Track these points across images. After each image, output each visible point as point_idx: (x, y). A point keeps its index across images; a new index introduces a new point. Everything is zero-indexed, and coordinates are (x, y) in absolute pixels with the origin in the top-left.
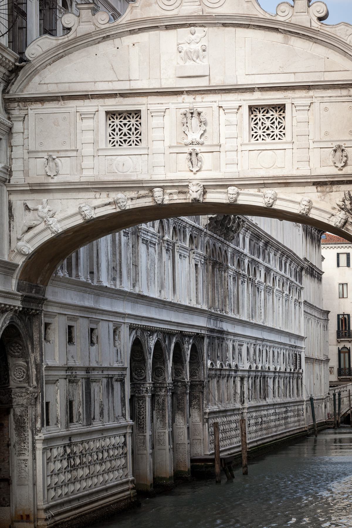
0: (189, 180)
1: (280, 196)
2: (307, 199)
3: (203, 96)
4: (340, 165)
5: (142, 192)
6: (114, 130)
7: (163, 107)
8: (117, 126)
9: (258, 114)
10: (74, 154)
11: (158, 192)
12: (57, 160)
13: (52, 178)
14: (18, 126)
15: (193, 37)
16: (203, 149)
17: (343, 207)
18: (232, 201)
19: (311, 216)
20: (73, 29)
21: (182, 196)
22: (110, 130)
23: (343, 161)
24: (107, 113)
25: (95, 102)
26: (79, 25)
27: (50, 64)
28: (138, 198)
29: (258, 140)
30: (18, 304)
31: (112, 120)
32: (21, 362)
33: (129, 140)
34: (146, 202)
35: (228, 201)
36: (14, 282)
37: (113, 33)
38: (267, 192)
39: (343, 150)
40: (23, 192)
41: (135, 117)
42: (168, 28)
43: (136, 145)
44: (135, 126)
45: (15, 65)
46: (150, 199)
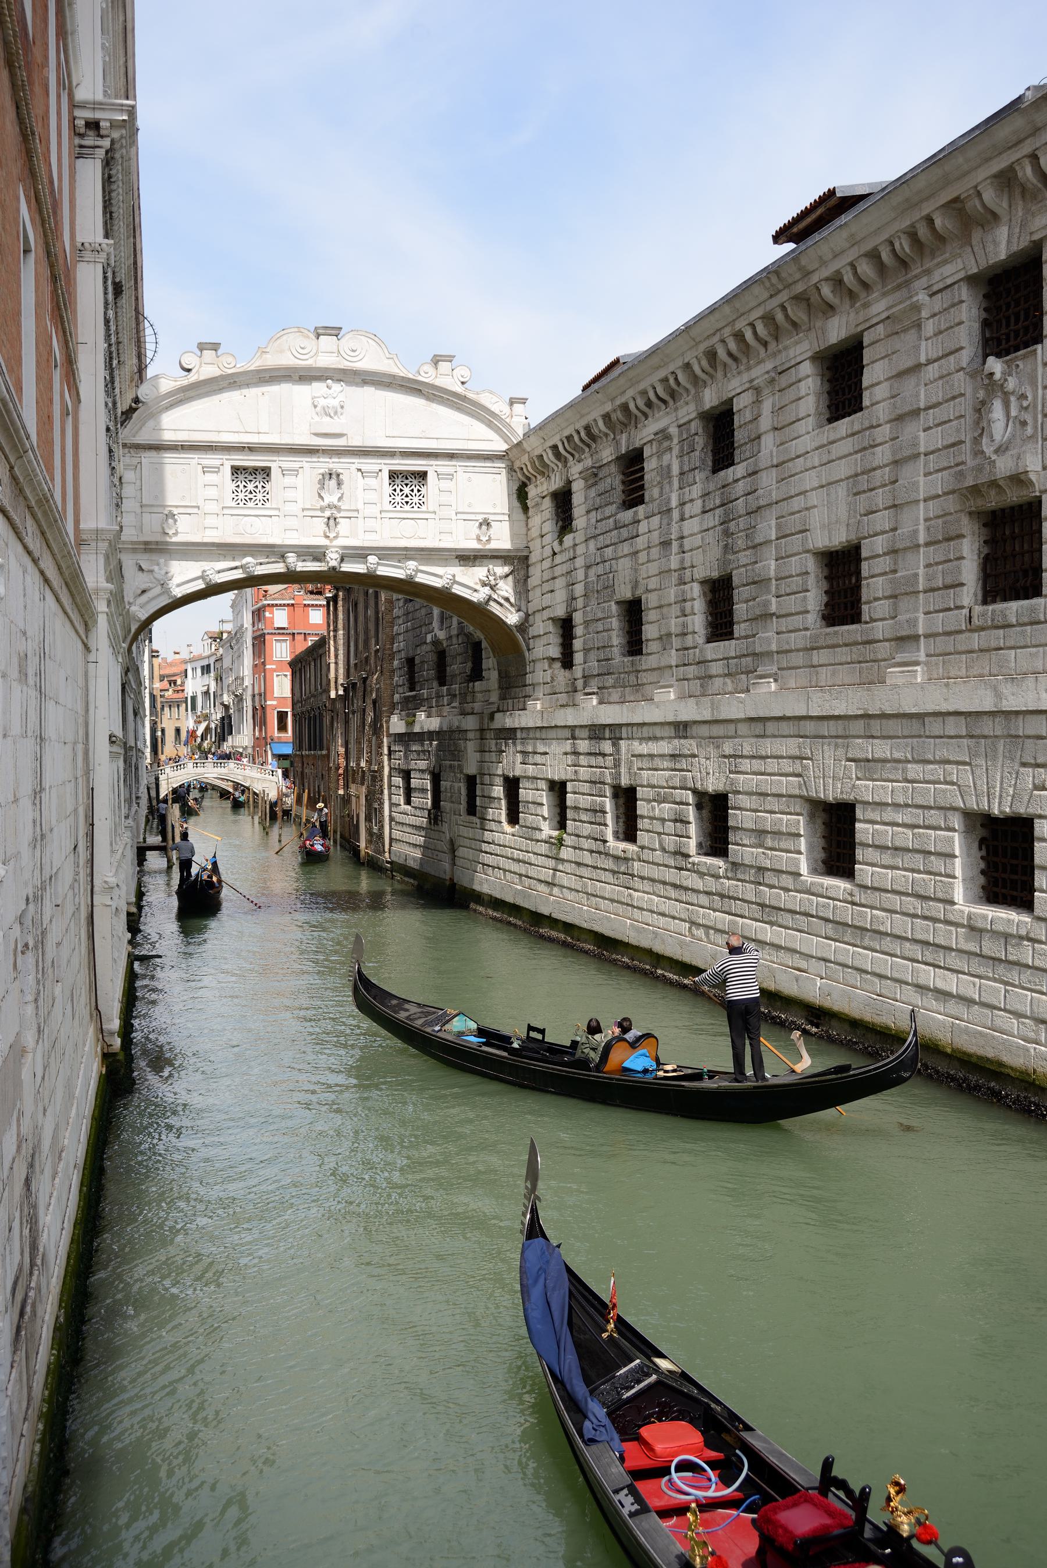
0: (326, 547)
4: (484, 539)
7: (296, 465)
10: (195, 510)
11: (291, 558)
14: (129, 476)
15: (331, 392)
16: (342, 514)
19: (453, 591)
21: (319, 564)
26: (200, 366)
28: (268, 563)
34: (279, 568)
39: (488, 524)
40: (134, 550)
46: (282, 565)
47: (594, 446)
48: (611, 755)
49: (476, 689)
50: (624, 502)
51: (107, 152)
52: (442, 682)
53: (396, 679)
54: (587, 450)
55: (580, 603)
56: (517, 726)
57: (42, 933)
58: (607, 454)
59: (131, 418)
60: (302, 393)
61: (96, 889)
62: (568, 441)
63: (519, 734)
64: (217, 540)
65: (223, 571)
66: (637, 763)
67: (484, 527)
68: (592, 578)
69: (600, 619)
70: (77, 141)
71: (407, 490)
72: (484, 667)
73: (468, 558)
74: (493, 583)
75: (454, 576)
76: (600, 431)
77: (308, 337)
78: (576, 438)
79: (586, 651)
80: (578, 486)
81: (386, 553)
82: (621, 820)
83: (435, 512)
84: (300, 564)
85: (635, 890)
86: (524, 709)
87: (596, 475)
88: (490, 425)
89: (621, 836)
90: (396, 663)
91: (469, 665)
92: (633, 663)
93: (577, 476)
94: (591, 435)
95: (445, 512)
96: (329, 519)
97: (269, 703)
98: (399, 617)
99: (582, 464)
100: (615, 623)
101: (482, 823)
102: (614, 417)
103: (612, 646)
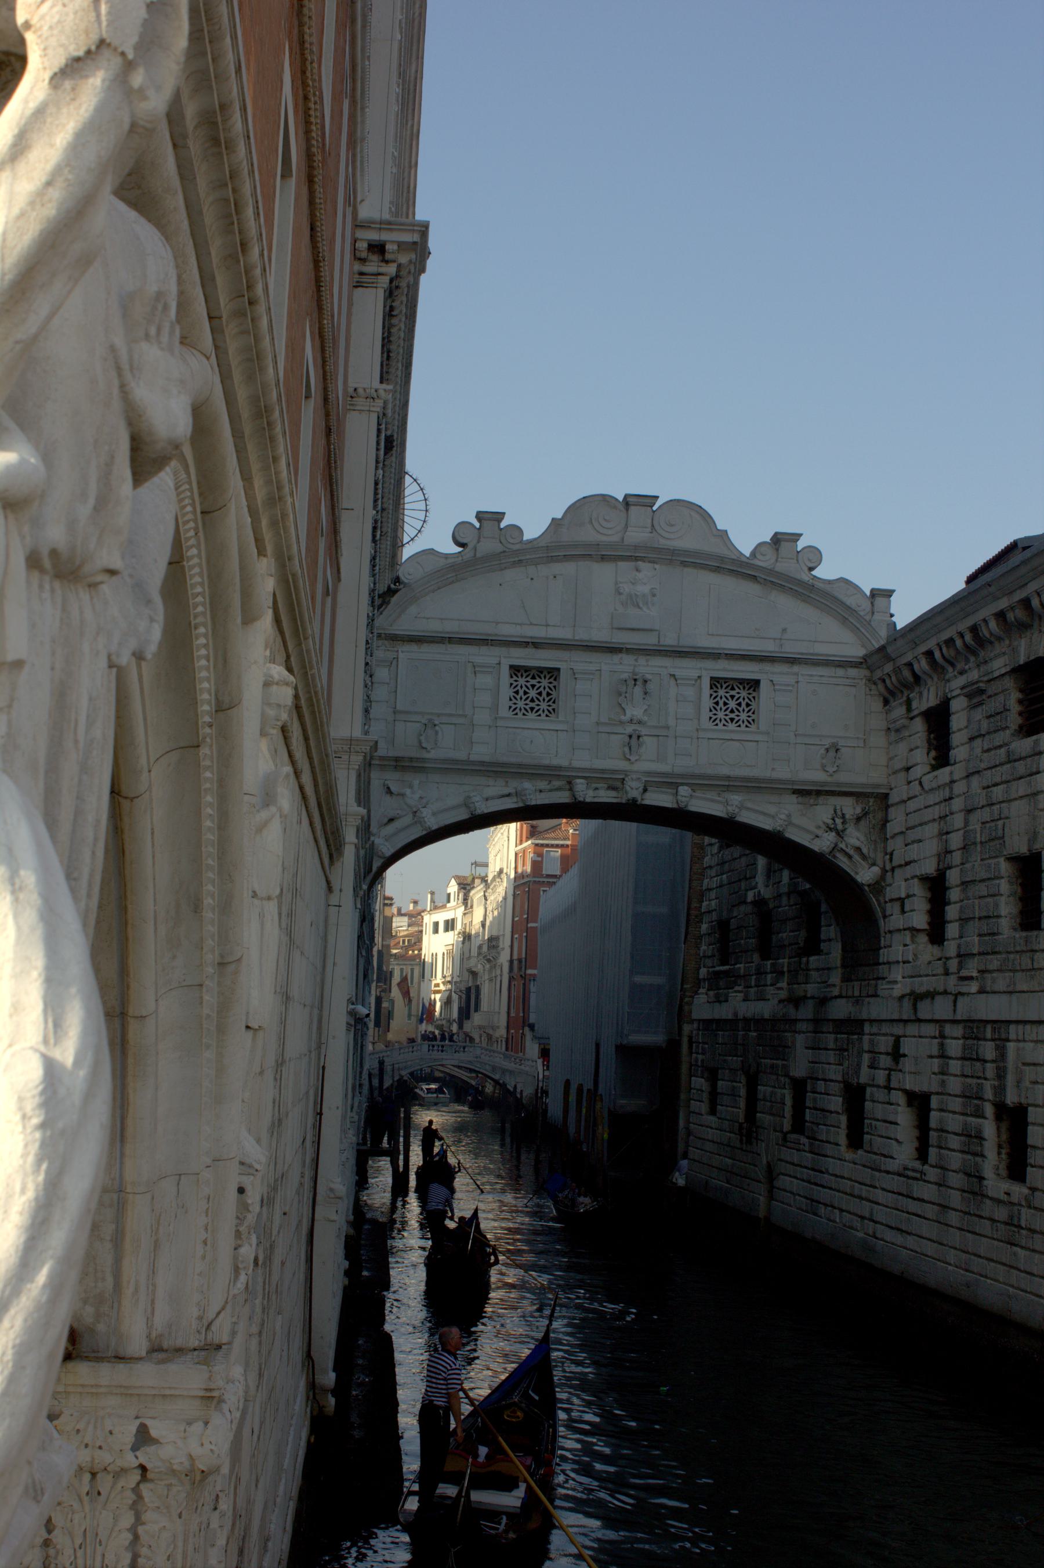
0: (626, 773)
1: (749, 805)
2: (787, 812)
3: (648, 657)
4: (831, 770)
5: (557, 783)
6: (517, 692)
8: (521, 687)
9: (719, 690)
10: (461, 721)
11: (580, 785)
12: (437, 728)
13: (429, 752)
15: (640, 576)
17: (832, 826)
18: (682, 805)
19: (787, 835)
20: (471, 546)
21: (613, 793)
22: (511, 692)
23: (836, 764)
24: (511, 667)
25: (497, 651)
26: (478, 542)
27: (433, 591)
28: (551, 790)
29: (717, 725)
31: (515, 678)
33: (537, 708)
34: (562, 797)
35: (675, 806)
37: (528, 557)
38: (732, 797)
39: (837, 750)
40: (382, 767)
41: (548, 677)
42: (604, 558)
43: (547, 716)
44: (547, 689)
45: (389, 587)
46: (567, 794)
47: (982, 654)
48: (993, 1061)
49: (811, 966)
50: (1021, 727)
51: (391, 281)
52: (765, 957)
53: (704, 948)
54: (972, 659)
55: (957, 858)
56: (865, 1017)
57: (271, 1246)
58: (999, 665)
59: (388, 603)
60: (603, 575)
61: (319, 1198)
62: (948, 647)
63: (867, 1028)
64: (487, 759)
65: (493, 798)
66: (1029, 1073)
67: (832, 753)
68: (975, 825)
69: (983, 881)
70: (357, 267)
71: (732, 704)
72: (823, 937)
73: (808, 793)
74: (840, 827)
75: (789, 816)
76: (991, 634)
77: (615, 507)
78: (959, 643)
79: (964, 921)
80: (958, 705)
81: (702, 782)
82: (1003, 1151)
83: (768, 733)
85: (1022, 1247)
86: (875, 995)
87: (982, 692)
88: (844, 621)
89: (1004, 1172)
90: (704, 927)
91: (803, 934)
92: (1027, 940)
93: (958, 692)
94: (979, 641)
96: (630, 736)
97: (529, 971)
98: (710, 867)
99: (965, 676)
100: (1004, 886)
101: (811, 1145)
102: (1010, 616)
103: (999, 917)
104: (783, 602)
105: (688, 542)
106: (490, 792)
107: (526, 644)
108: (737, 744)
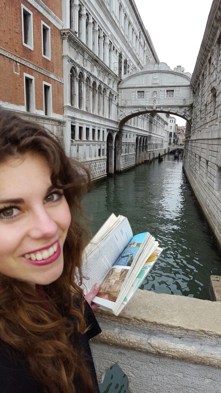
5: (144, 108)
11: (147, 108)
14: (120, 94)
21: (152, 109)
24: (138, 91)
25: (135, 89)
30: (118, 130)
32: (118, 141)
34: (144, 110)
36: (118, 126)
40: (120, 108)
42: (151, 73)
51: (68, 38)
60: (151, 76)
64: (134, 105)
71: (170, 94)
73: (181, 107)
81: (164, 107)
84: (149, 109)
95: (177, 98)
104: (178, 77)
105: (163, 69)
106: (135, 110)
107: (139, 88)
108: (170, 100)
